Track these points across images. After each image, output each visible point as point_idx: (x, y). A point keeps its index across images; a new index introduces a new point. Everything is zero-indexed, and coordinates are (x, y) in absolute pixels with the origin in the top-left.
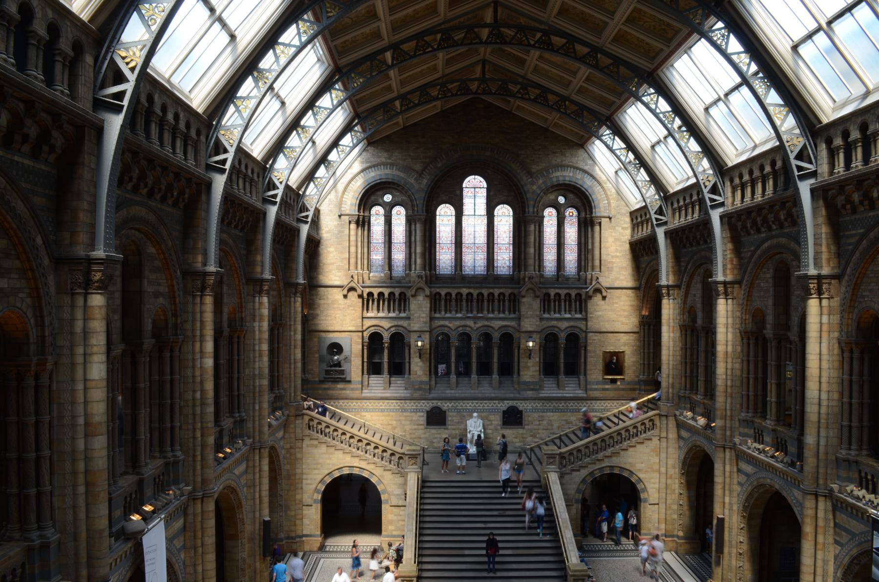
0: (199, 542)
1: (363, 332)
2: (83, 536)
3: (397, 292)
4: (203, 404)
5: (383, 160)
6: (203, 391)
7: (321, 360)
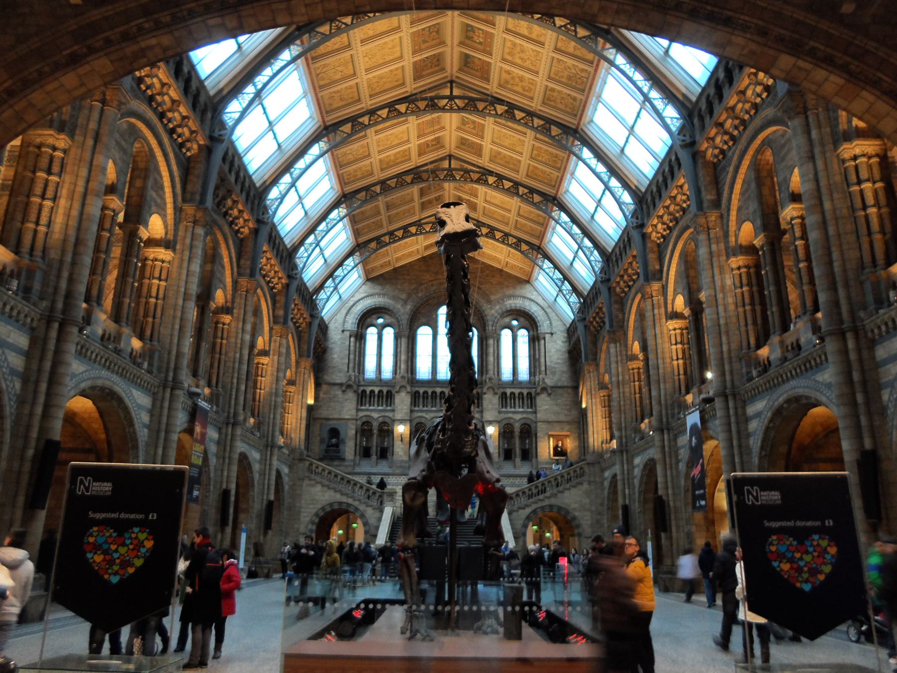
0: (227, 454)
1: (356, 420)
2: (174, 353)
3: (385, 390)
4: (240, 362)
5: (378, 291)
6: (241, 355)
7: (322, 441)
